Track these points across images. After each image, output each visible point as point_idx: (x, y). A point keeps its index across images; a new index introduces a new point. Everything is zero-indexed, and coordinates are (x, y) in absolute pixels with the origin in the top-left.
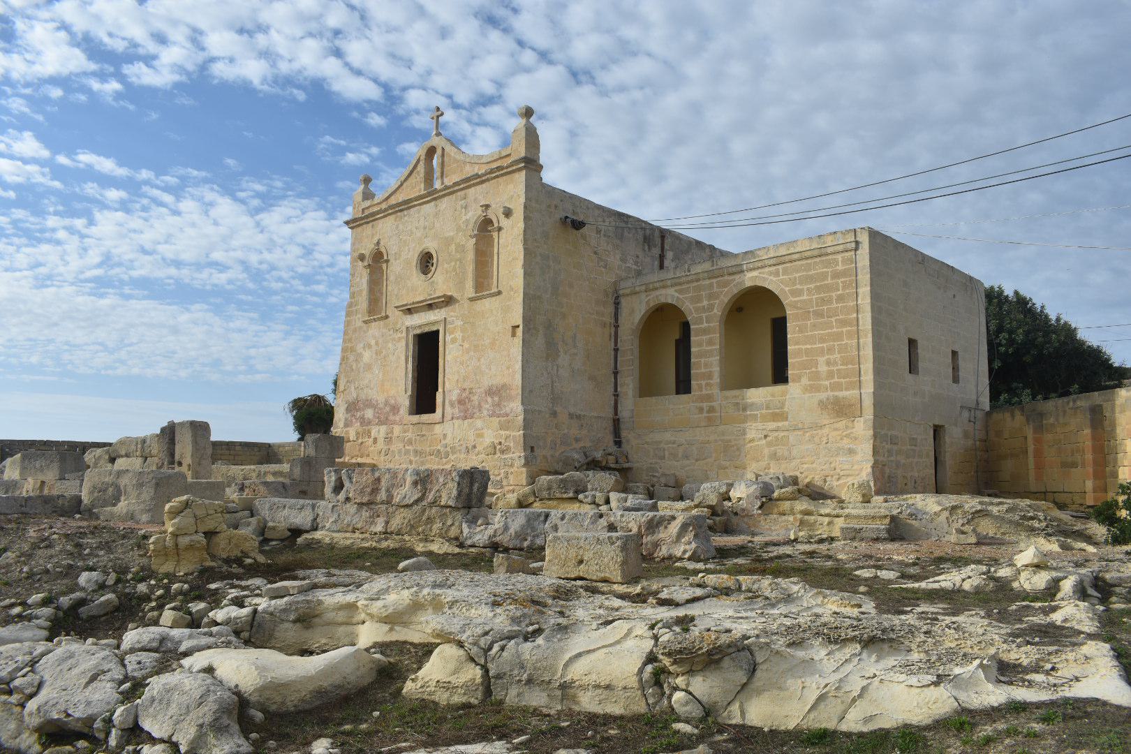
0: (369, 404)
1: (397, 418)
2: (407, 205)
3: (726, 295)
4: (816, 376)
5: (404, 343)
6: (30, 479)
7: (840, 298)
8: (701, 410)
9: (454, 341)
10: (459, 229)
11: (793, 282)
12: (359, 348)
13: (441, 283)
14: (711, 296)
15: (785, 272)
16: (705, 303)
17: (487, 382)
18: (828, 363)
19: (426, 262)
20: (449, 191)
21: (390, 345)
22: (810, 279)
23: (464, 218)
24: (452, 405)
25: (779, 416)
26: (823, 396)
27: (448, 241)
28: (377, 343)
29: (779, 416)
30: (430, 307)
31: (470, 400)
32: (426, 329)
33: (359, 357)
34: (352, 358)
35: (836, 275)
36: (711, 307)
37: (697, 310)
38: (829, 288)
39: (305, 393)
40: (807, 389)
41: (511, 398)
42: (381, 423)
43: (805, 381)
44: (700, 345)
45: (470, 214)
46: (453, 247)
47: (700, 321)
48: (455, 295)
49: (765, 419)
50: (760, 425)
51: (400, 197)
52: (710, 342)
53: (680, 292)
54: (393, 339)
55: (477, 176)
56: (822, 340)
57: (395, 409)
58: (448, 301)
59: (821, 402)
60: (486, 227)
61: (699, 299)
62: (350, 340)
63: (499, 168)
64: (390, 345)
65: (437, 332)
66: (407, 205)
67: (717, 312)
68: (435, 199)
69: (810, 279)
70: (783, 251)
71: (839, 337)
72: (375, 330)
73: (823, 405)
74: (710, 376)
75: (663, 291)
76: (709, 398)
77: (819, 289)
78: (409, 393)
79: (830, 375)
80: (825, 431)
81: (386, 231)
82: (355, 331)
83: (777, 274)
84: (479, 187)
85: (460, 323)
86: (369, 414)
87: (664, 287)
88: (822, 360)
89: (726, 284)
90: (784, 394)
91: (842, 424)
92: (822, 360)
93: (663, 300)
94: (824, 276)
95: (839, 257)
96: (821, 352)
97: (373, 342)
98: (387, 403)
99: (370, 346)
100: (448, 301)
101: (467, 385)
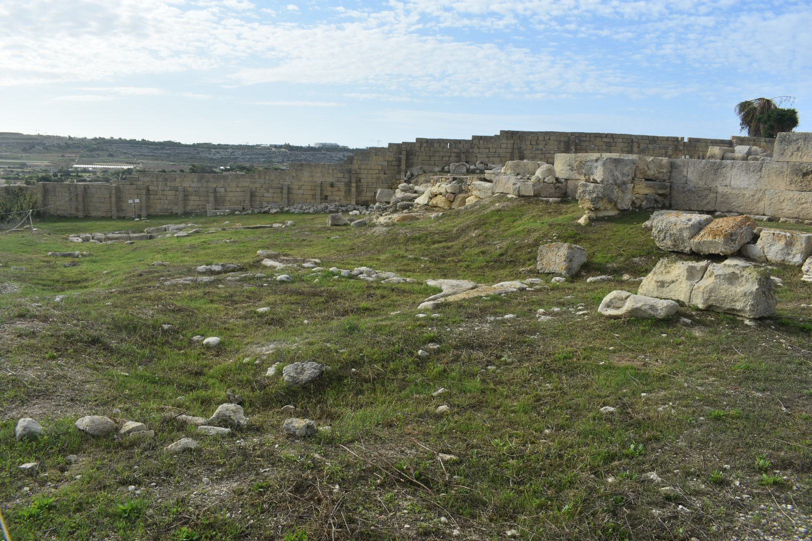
39: (752, 96)
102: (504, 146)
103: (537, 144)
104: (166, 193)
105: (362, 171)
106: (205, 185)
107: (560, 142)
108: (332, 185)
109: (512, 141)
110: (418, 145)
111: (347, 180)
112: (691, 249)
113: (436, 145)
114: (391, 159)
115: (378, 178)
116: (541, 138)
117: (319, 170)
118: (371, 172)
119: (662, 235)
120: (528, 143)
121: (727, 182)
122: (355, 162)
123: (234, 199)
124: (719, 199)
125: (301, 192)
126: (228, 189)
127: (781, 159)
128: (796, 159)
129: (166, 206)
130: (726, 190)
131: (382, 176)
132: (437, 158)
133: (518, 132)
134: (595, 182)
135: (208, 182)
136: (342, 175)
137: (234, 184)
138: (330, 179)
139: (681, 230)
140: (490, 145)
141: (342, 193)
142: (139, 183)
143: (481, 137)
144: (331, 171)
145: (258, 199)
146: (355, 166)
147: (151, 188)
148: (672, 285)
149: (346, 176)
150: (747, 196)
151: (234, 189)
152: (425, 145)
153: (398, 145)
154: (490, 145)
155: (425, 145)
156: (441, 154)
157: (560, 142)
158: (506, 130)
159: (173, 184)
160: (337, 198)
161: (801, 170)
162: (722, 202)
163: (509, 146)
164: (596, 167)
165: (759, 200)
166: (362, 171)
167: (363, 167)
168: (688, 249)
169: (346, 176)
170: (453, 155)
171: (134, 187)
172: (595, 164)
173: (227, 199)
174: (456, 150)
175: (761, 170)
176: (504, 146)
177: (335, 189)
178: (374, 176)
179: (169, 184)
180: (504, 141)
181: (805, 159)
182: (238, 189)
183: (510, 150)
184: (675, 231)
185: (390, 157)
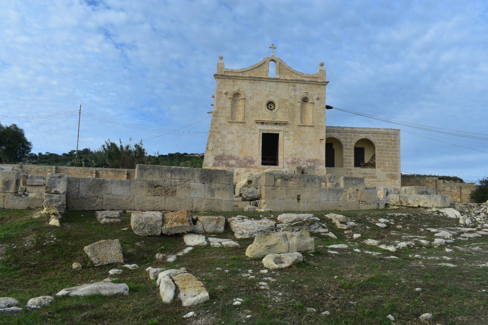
0: (231, 157)
1: (253, 166)
2: (260, 79)
3: (357, 139)
4: (385, 167)
5: (257, 136)
6: (350, 188)
7: (392, 147)
8: (347, 173)
9: (288, 139)
10: (291, 97)
11: (379, 140)
12: (224, 132)
13: (280, 115)
14: (351, 139)
15: (376, 136)
16: (349, 140)
17: (307, 157)
18: (389, 164)
19: (270, 105)
20: (286, 81)
21: (247, 135)
22: (384, 140)
23: (293, 94)
24: (288, 163)
25: (374, 177)
26: (387, 173)
27: (285, 101)
28: (238, 132)
29: (374, 177)
30: (276, 124)
31: (298, 163)
32: (271, 132)
33: (223, 137)
34: (218, 136)
35: (391, 141)
36: (351, 142)
37: (346, 142)
38: (389, 144)
40: (382, 170)
41: (320, 164)
42: (241, 166)
43: (382, 168)
44: (347, 152)
45: (296, 94)
46: (288, 103)
47: (347, 145)
48: (289, 122)
49: (369, 178)
50: (368, 179)
51: (253, 75)
52: (350, 153)
53: (339, 135)
54: (249, 133)
55: (305, 81)
56: (387, 157)
57: (251, 162)
58: (285, 124)
59: (387, 174)
60: (305, 100)
61: (347, 138)
62: (217, 128)
63: (315, 81)
64: (247, 135)
65: (278, 134)
66: (260, 79)
67: (353, 144)
68: (277, 82)
69: (384, 140)
70: (376, 130)
71: (392, 157)
72: (235, 128)
73: (387, 175)
74: (350, 163)
75: (333, 133)
76: (350, 170)
77: (386, 143)
78: (261, 156)
79: (389, 167)
80: (388, 182)
81: (244, 86)
82: (221, 124)
83: (374, 136)
84: (302, 85)
85: (292, 133)
86: (232, 162)
87: (334, 132)
88: (387, 163)
89: (357, 136)
90: (375, 171)
91: (393, 181)
92: (387, 163)
93: (333, 136)
94: (388, 140)
95: (393, 136)
96: (387, 161)
97: (235, 132)
98: (245, 159)
99: (232, 133)
100: (285, 124)
101: (296, 157)
112: (162, 233)
119: (142, 227)
121: (109, 192)
124: (105, 202)
127: (141, 179)
128: (150, 178)
130: (109, 196)
134: (57, 193)
139: (156, 222)
148: (275, 247)
150: (123, 199)
161: (153, 185)
162: (107, 204)
164: (59, 182)
165: (131, 202)
168: (159, 233)
172: (58, 180)
175: (130, 185)
181: (154, 179)
184: (152, 223)
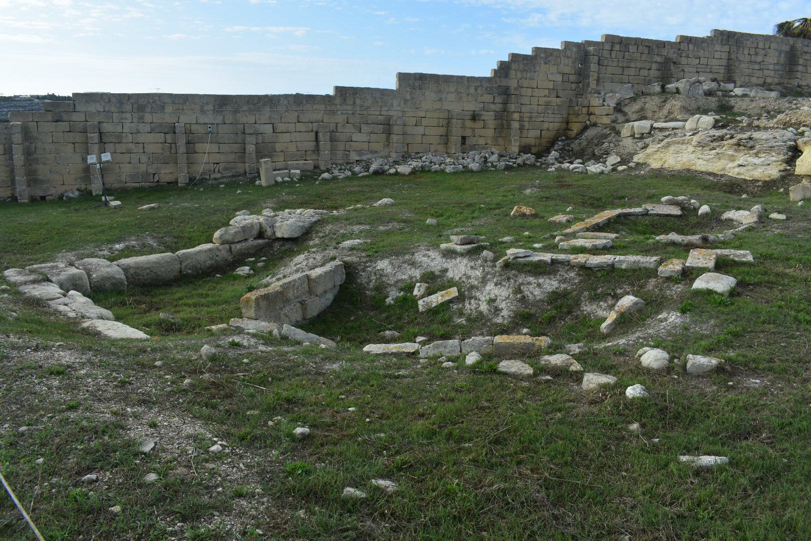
102: (717, 55)
103: (757, 54)
104: (141, 138)
105: (523, 91)
106: (229, 118)
107: (780, 52)
108: (474, 117)
109: (726, 48)
110: (608, 47)
111: (498, 107)
113: (632, 49)
114: (567, 70)
115: (547, 104)
116: (761, 45)
117: (452, 89)
118: (537, 92)
120: (746, 52)
122: (512, 73)
123: (292, 148)
125: (420, 130)
126: (281, 127)
129: (143, 168)
131: (554, 101)
132: (632, 72)
133: (735, 33)
135: (236, 112)
136: (488, 98)
137: (292, 117)
138: (471, 106)
140: (701, 53)
141: (490, 132)
142: (75, 117)
143: (691, 38)
144: (472, 90)
145: (341, 146)
146: (513, 84)
147: (107, 127)
149: (499, 99)
151: (291, 127)
152: (617, 47)
153: (578, 45)
154: (701, 53)
155: (617, 47)
156: (639, 65)
157: (780, 52)
158: (721, 29)
159: (157, 118)
160: (482, 141)
163: (725, 56)
166: (523, 91)
167: (525, 83)
169: (499, 99)
170: (654, 66)
171: (64, 126)
173: (278, 147)
174: (658, 59)
176: (717, 55)
177: (480, 124)
178: (542, 101)
179: (148, 117)
180: (718, 47)
182: (300, 127)
183: (724, 62)
185: (567, 66)
